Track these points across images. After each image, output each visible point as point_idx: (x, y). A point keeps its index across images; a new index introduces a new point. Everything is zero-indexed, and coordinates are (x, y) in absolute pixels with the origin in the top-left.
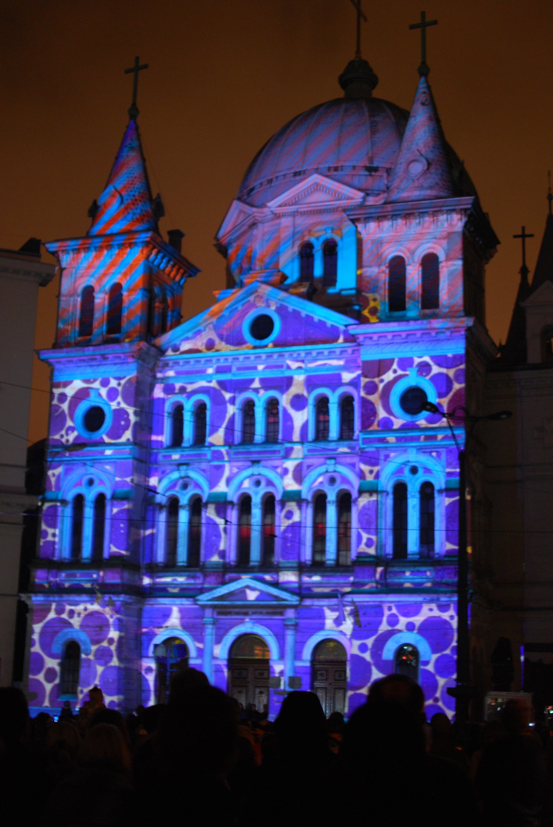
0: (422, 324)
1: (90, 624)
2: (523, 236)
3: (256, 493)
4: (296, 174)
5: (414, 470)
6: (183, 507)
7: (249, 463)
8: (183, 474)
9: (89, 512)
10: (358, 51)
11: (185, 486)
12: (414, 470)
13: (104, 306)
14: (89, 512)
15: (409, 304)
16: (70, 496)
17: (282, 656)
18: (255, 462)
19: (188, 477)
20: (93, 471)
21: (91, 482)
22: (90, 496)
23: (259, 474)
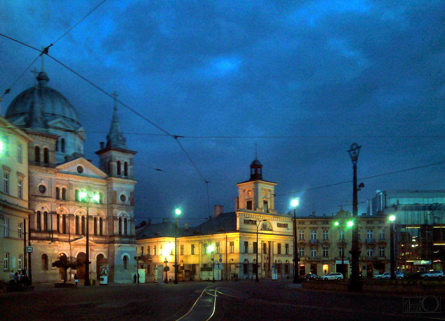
6: (61, 217)
7: (79, 207)
9: (42, 216)
12: (123, 215)
14: (42, 216)
18: (81, 207)
20: (45, 205)
21: (43, 208)
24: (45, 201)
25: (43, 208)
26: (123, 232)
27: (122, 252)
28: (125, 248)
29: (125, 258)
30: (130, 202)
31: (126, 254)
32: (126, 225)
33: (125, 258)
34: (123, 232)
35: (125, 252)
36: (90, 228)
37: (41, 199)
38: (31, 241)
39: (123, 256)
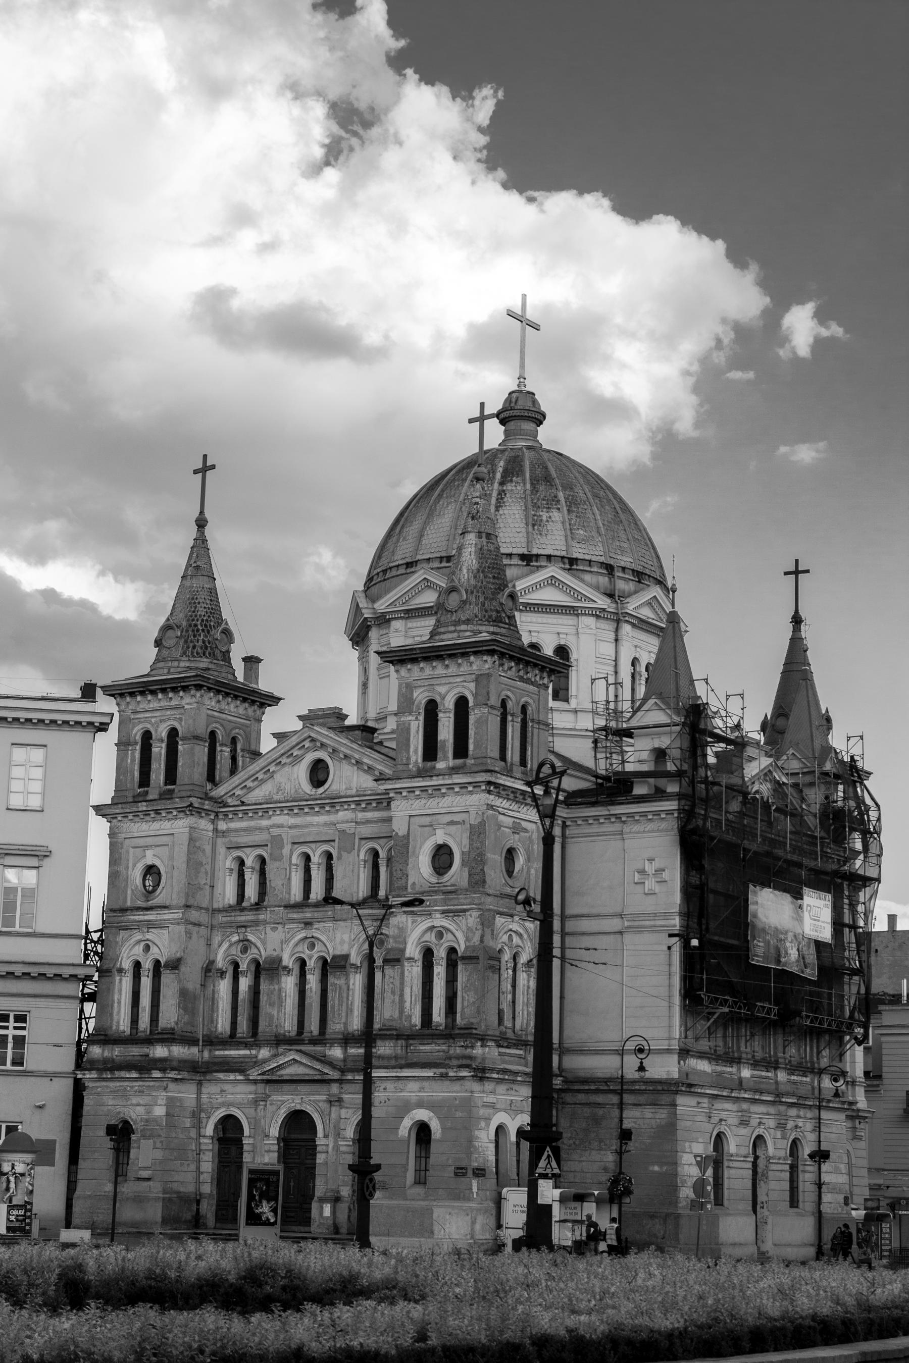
0: (443, 779)
1: (141, 1102)
2: (797, 572)
3: (310, 958)
4: (409, 565)
5: (440, 935)
6: (245, 973)
7: (302, 926)
8: (242, 938)
9: (146, 982)
10: (522, 377)
11: (245, 950)
12: (440, 935)
13: (161, 754)
14: (146, 982)
15: (440, 755)
16: (127, 964)
17: (326, 1136)
19: (248, 940)
21: (147, 948)
22: (147, 965)
23: (313, 937)
24: (150, 925)
25: (147, 948)
26: (438, 1015)
27: (406, 1107)
28: (422, 1089)
29: (423, 1131)
30: (466, 874)
31: (422, 1114)
32: (451, 980)
33: (423, 1131)
34: (438, 1015)
35: (420, 1105)
36: (333, 1007)
37: (136, 918)
38: (88, 1076)
39: (407, 1123)
